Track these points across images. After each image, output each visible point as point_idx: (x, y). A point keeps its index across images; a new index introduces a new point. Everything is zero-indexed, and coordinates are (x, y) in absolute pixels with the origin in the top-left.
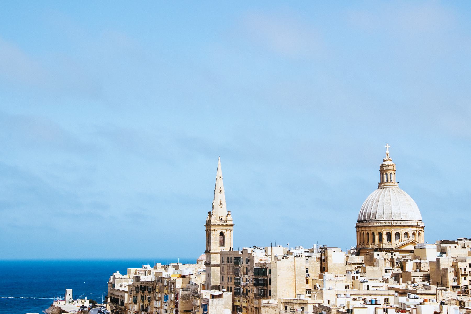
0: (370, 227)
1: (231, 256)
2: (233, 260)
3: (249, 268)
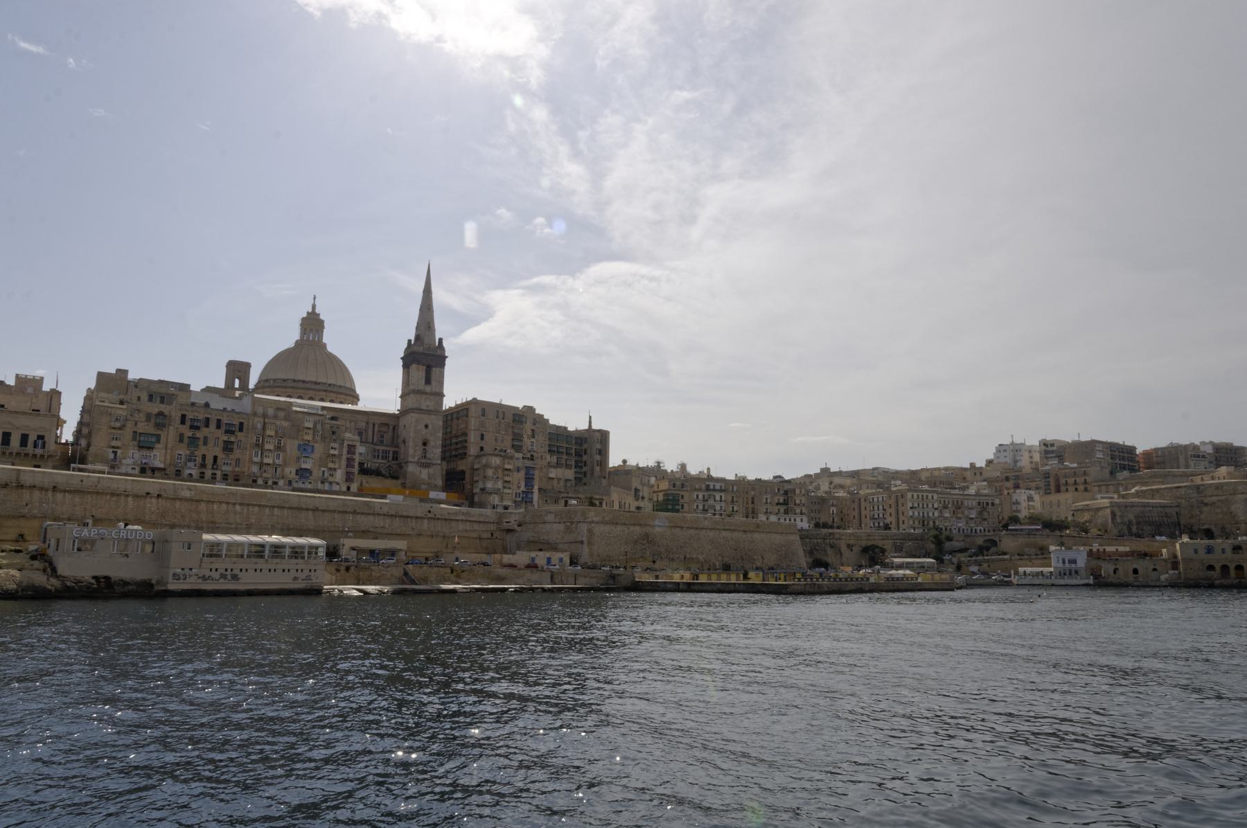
0: (341, 393)
2: (509, 418)
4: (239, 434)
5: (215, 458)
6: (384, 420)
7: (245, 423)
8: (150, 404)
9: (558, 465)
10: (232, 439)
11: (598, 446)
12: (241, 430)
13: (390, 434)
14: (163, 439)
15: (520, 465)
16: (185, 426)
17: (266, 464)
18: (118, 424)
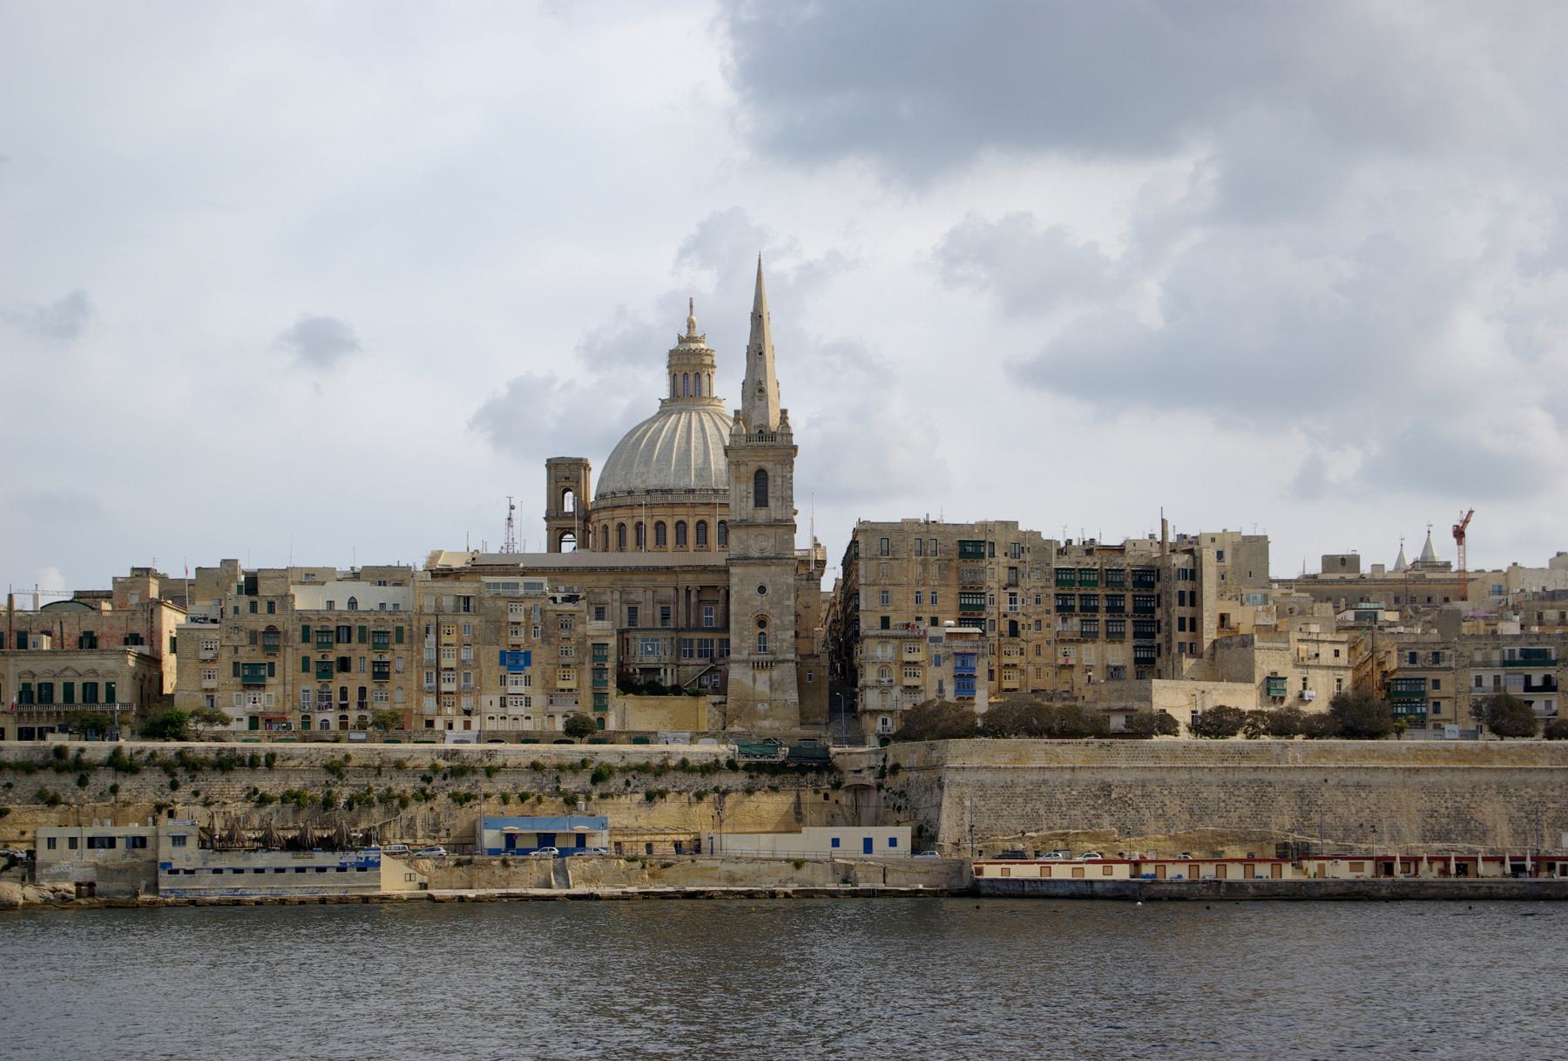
3: (1021, 567)
4: (396, 647)
5: (362, 690)
6: (707, 579)
7: (406, 628)
8: (253, 617)
9: (1087, 637)
10: (387, 658)
11: (1184, 586)
12: (400, 640)
13: (721, 605)
14: (278, 669)
15: (941, 651)
16: (309, 645)
17: (446, 693)
18: (209, 655)
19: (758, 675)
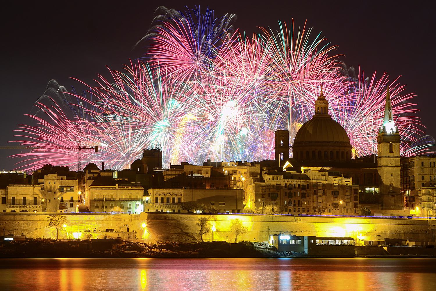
1: (434, 162)
4: (307, 189)
12: (308, 188)
14: (279, 196)
19: (391, 198)
